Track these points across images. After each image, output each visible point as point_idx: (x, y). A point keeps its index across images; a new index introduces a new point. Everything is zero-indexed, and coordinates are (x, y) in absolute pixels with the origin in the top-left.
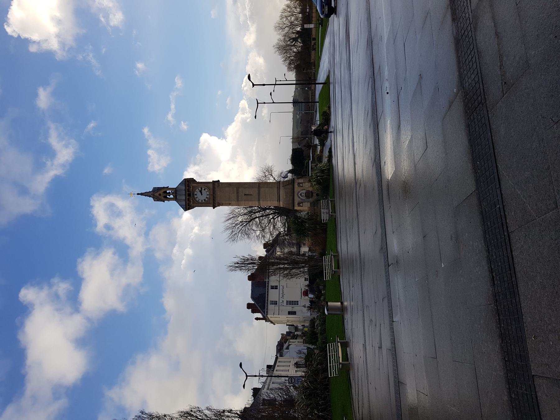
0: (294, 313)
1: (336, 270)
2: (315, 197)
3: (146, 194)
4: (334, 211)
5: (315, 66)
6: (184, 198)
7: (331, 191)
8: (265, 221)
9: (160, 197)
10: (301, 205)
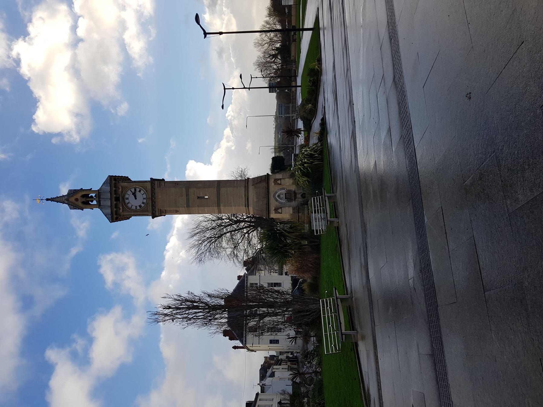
0: (277, 342)
1: (349, 332)
2: (300, 199)
3: (59, 199)
4: (335, 213)
5: (295, 62)
6: (109, 203)
7: (326, 183)
8: (238, 236)
9: (76, 203)
10: (280, 211)
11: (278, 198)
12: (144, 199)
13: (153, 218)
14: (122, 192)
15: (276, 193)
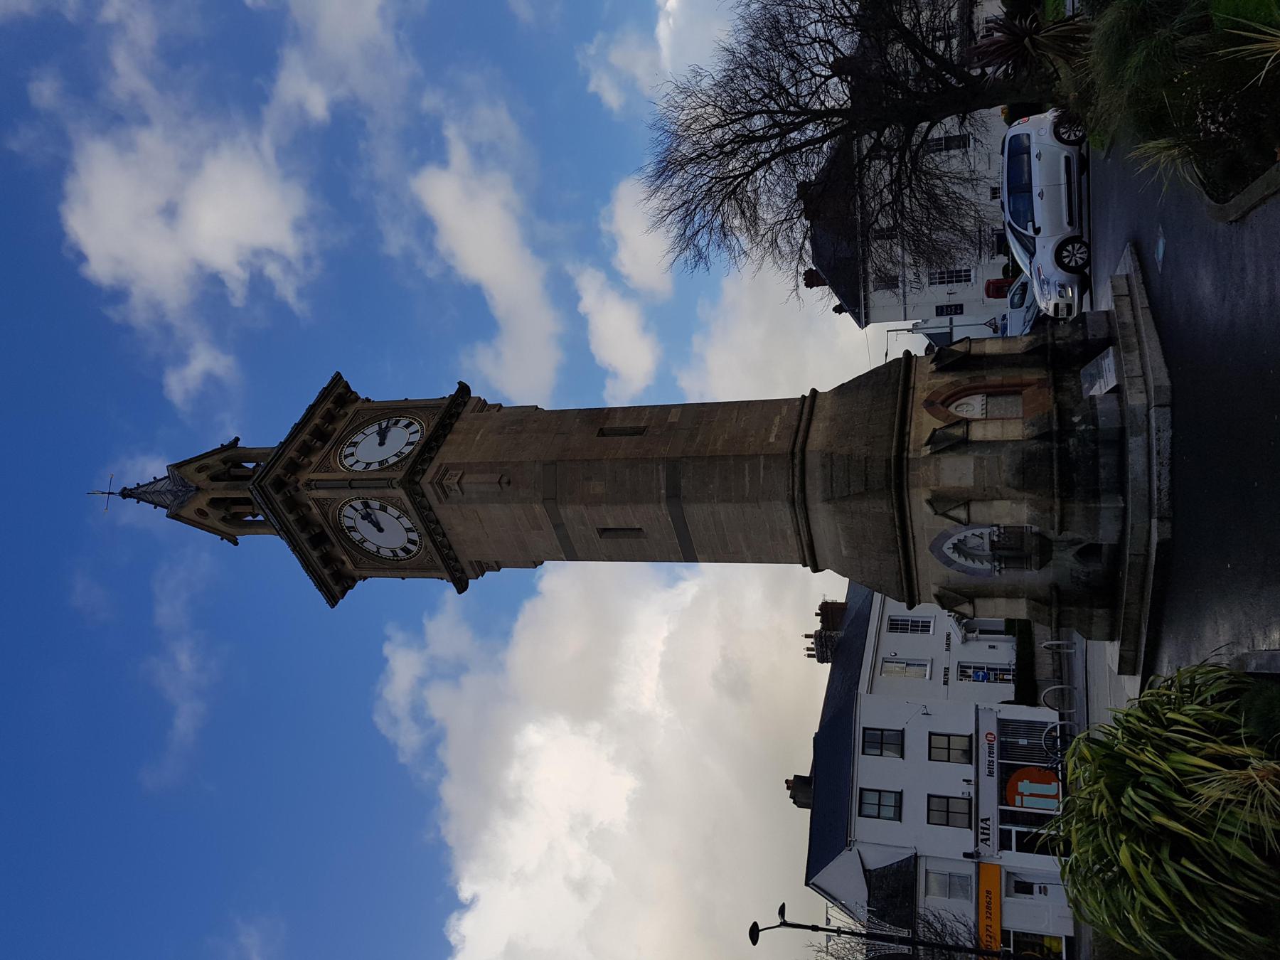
11: (955, 556)
12: (408, 530)
13: (462, 587)
14: (325, 515)
15: (946, 536)
